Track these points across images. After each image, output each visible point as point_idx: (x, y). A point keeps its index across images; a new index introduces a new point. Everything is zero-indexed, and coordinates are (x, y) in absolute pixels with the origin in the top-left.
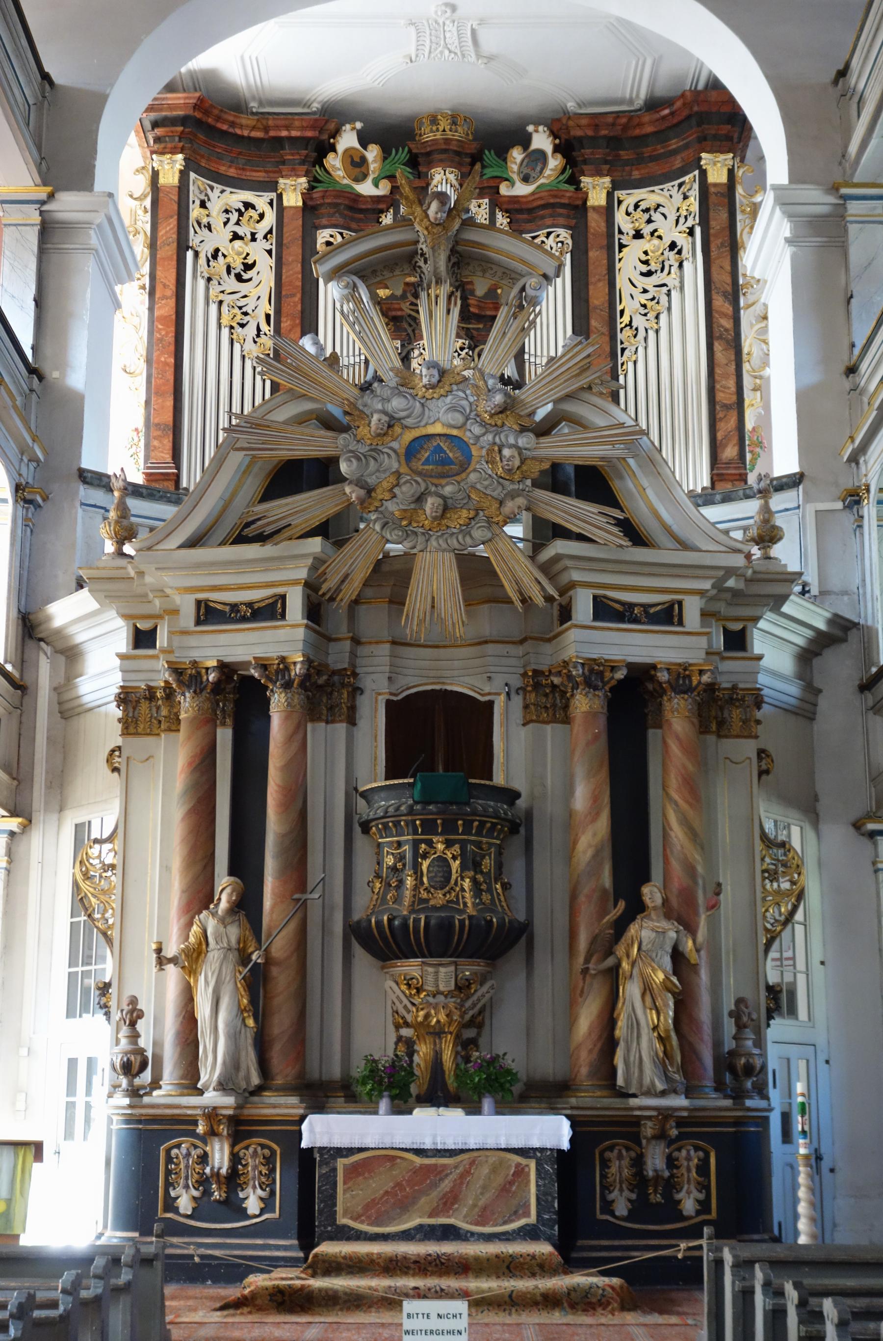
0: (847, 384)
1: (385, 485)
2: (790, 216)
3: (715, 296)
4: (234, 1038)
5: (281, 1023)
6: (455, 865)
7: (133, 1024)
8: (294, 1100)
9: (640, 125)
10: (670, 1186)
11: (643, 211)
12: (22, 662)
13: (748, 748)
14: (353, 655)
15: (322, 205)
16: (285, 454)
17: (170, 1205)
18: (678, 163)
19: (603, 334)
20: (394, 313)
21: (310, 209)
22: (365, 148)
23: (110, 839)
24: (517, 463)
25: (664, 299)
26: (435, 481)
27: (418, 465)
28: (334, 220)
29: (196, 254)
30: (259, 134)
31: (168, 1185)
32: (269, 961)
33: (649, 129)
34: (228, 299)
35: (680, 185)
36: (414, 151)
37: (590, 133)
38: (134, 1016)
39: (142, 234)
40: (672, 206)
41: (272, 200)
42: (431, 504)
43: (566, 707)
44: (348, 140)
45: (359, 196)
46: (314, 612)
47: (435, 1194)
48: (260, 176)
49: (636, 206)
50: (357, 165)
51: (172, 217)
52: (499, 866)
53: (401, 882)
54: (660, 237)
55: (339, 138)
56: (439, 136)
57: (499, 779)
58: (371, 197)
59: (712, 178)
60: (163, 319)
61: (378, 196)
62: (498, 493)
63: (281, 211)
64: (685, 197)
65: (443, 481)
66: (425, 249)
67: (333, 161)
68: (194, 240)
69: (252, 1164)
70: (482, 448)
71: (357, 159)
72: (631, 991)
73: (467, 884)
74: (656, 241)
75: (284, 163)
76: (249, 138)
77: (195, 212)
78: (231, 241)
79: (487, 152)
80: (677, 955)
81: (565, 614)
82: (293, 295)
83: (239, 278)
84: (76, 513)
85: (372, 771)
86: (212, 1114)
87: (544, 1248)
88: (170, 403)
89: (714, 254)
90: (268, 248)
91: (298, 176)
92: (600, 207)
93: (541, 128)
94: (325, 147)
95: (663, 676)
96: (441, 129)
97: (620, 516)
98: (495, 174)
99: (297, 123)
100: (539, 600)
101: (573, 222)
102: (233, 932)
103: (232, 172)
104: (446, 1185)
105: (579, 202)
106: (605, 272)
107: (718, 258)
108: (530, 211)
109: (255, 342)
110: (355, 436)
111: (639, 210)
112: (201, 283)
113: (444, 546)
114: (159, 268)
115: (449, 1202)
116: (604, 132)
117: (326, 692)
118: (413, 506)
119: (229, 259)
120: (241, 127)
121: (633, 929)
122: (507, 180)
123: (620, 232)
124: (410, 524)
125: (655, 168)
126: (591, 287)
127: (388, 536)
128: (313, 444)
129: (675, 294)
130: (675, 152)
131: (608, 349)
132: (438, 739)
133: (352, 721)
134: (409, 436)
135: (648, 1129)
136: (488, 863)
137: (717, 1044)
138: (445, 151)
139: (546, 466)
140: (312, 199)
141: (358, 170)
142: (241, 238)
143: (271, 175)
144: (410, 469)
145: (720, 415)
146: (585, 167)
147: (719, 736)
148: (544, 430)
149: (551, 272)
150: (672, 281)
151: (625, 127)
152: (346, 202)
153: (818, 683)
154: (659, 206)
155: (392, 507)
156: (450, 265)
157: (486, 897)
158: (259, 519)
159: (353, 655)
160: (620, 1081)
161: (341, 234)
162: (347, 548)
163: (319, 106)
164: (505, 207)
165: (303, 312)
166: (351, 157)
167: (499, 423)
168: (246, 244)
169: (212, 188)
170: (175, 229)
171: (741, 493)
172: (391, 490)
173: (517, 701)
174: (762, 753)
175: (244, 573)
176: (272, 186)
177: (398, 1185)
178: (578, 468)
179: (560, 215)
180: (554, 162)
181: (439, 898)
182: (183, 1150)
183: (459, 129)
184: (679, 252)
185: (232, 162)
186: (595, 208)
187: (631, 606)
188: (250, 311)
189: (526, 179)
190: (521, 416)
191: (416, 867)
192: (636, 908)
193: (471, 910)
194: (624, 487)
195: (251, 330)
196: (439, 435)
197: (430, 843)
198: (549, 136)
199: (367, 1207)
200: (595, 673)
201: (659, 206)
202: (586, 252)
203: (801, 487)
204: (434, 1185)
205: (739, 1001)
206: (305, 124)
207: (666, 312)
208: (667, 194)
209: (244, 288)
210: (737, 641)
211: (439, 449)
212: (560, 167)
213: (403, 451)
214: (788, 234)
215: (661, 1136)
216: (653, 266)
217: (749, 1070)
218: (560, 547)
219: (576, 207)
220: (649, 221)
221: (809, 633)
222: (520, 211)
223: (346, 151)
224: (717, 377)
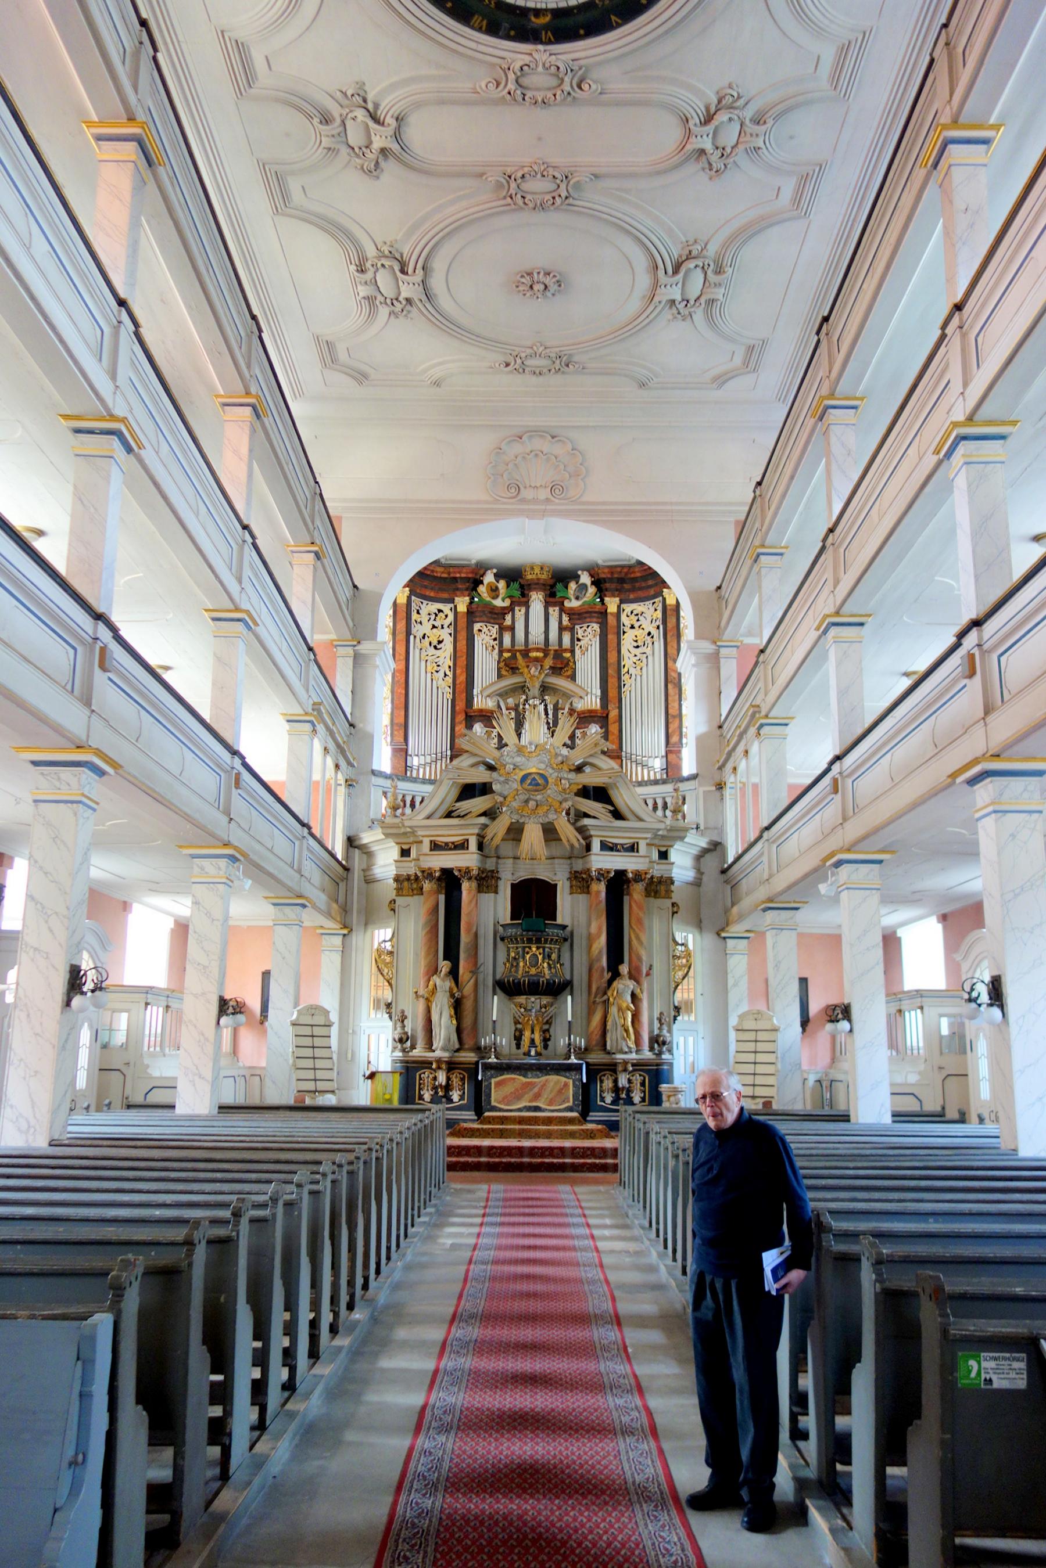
0: (718, 732)
2: (695, 653)
4: (447, 1028)
5: (467, 1021)
6: (540, 957)
7: (403, 1021)
8: (472, 1055)
9: (634, 572)
10: (629, 1091)
12: (347, 856)
13: (668, 903)
14: (497, 863)
17: (421, 1098)
18: (652, 592)
21: (472, 614)
23: (390, 940)
25: (645, 660)
27: (526, 786)
30: (445, 575)
31: (420, 1089)
32: (463, 997)
33: (638, 575)
38: (403, 1019)
40: (648, 612)
42: (532, 804)
43: (588, 887)
44: (489, 578)
46: (480, 847)
47: (531, 1094)
48: (446, 596)
50: (494, 591)
52: (559, 957)
53: (518, 964)
56: (534, 577)
57: (559, 920)
59: (668, 602)
60: (399, 671)
62: (560, 798)
63: (456, 613)
67: (482, 589)
68: (414, 630)
69: (456, 1081)
72: (613, 1010)
73: (545, 965)
74: (641, 631)
75: (457, 589)
80: (633, 996)
81: (588, 848)
83: (435, 647)
85: (504, 913)
86: (439, 1061)
87: (575, 1114)
88: (403, 713)
94: (478, 582)
95: (630, 875)
100: (576, 845)
102: (449, 983)
103: (432, 594)
104: (536, 1090)
108: (579, 614)
112: (417, 651)
115: (537, 1097)
117: (486, 881)
121: (615, 984)
125: (640, 594)
128: (480, 776)
129: (650, 658)
130: (650, 587)
132: (534, 901)
133: (496, 892)
134: (522, 773)
135: (620, 1068)
136: (554, 956)
137: (651, 1031)
138: (537, 584)
139: (580, 787)
145: (670, 720)
147: (655, 897)
148: (579, 769)
151: (626, 574)
153: (702, 870)
155: (514, 804)
157: (553, 971)
159: (497, 863)
160: (608, 1048)
173: (568, 884)
174: (673, 904)
175: (450, 831)
177: (517, 1090)
180: (592, 590)
181: (533, 971)
182: (427, 1075)
187: (616, 845)
189: (577, 598)
191: (524, 957)
192: (615, 975)
193: (548, 977)
197: (530, 948)
199: (504, 1099)
200: (602, 874)
204: (531, 1090)
205: (661, 1013)
210: (664, 855)
211: (534, 779)
214: (693, 662)
215: (625, 1070)
216: (640, 643)
217: (664, 1043)
218: (586, 821)
219: (601, 613)
221: (699, 849)
223: (488, 584)
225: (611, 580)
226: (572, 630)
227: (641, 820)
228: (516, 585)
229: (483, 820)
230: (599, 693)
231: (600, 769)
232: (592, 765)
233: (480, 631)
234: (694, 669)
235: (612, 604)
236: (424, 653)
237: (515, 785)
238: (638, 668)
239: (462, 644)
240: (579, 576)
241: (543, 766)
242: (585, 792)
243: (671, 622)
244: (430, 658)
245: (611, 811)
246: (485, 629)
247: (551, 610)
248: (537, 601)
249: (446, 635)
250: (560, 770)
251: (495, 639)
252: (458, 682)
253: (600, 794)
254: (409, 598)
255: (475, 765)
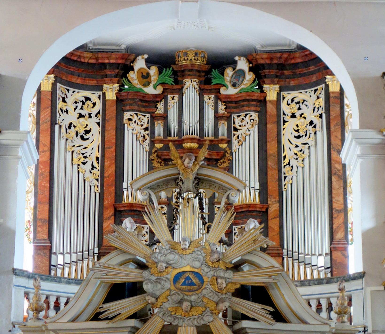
1: (164, 295)
2: (360, 144)
3: (332, 152)
9: (294, 58)
11: (296, 103)
15: (126, 99)
16: (118, 280)
18: (314, 79)
19: (275, 169)
20: (164, 157)
22: (149, 69)
24: (224, 285)
25: (306, 151)
26: (187, 293)
27: (179, 285)
28: (132, 108)
29: (60, 126)
30: (93, 61)
33: (299, 60)
34: (76, 149)
35: (316, 91)
36: (175, 69)
37: (268, 62)
39: (32, 117)
41: (100, 96)
42: (186, 305)
44: (140, 64)
45: (147, 94)
48: (93, 83)
49: (293, 100)
50: (145, 77)
51: (48, 108)
54: (305, 118)
55: (135, 63)
56: (188, 62)
58: (152, 95)
59: (331, 89)
60: (43, 163)
61: (156, 95)
62: (216, 299)
63: (104, 102)
64: (318, 98)
65: (191, 293)
66: (182, 178)
67: (132, 75)
68: (59, 120)
70: (208, 278)
71: (145, 74)
74: (302, 120)
75: (106, 76)
76: (88, 63)
77: (60, 104)
78: (78, 118)
79: (213, 70)
82: (112, 148)
83: (82, 138)
84: (12, 290)
88: (47, 207)
89: (332, 129)
90: (98, 122)
91: (114, 83)
92: (273, 101)
93: (242, 58)
96: (189, 59)
97: (272, 310)
98: (218, 82)
99: (114, 56)
101: (259, 109)
103: (79, 81)
105: (262, 99)
106: (275, 136)
107: (335, 131)
108: (236, 102)
109: (91, 172)
110: (150, 272)
111: (294, 102)
112: (63, 142)
113: (191, 324)
114: (41, 135)
116: (275, 61)
118: (176, 305)
119: (77, 129)
120: (84, 58)
122: (224, 86)
123: (284, 114)
124: (175, 314)
125: (302, 81)
126: (268, 144)
127: (165, 320)
128: (131, 274)
129: (312, 149)
130: (312, 73)
131: (277, 177)
138: (192, 70)
139: (238, 286)
140: (121, 96)
141: (145, 80)
142: (84, 116)
143: (99, 82)
144: (175, 287)
145: (335, 216)
146: (265, 79)
148: (237, 267)
149: (240, 188)
150: (311, 141)
151: (286, 59)
152: (139, 98)
154: (304, 101)
156: (194, 185)
158: (106, 311)
161: (136, 114)
162: (147, 324)
163: (125, 46)
164: (223, 100)
165: (116, 156)
166: (142, 73)
167: (216, 266)
168: (86, 120)
169: (68, 90)
170: (50, 115)
171: (336, 280)
172: (167, 298)
176: (100, 88)
178: (252, 286)
179: (252, 105)
180: (250, 76)
183: (199, 59)
184: (315, 127)
185: (79, 76)
186: (270, 101)
188: (88, 156)
189: (234, 85)
190: (226, 263)
194: (274, 294)
195: (88, 166)
196: (189, 272)
198: (246, 62)
201: (304, 101)
202: (266, 124)
203: (364, 279)
206: (117, 57)
207: (308, 158)
208: (309, 95)
209: (85, 143)
211: (188, 278)
212: (252, 80)
213: (172, 279)
214: (358, 152)
216: (301, 133)
218: (245, 324)
219: (260, 101)
220: (299, 109)
222: (231, 102)
224: (333, 195)
225: (270, 66)
226: (228, 119)
227: (304, 322)
228: (169, 72)
229: (133, 322)
230: (258, 186)
231: (258, 267)
232: (251, 263)
233: (130, 120)
234: (360, 160)
235: (271, 92)
236: (70, 144)
237: (168, 285)
238: (300, 159)
239: (111, 134)
240: (235, 62)
241: (197, 264)
242: (243, 292)
243: (335, 110)
244: (76, 149)
245: (271, 313)
246: (135, 118)
247: (206, 98)
248: (191, 89)
249: (92, 124)
250: (216, 269)
251: (146, 129)
252: (106, 175)
253: (259, 294)
254: (54, 85)
255: (123, 263)
